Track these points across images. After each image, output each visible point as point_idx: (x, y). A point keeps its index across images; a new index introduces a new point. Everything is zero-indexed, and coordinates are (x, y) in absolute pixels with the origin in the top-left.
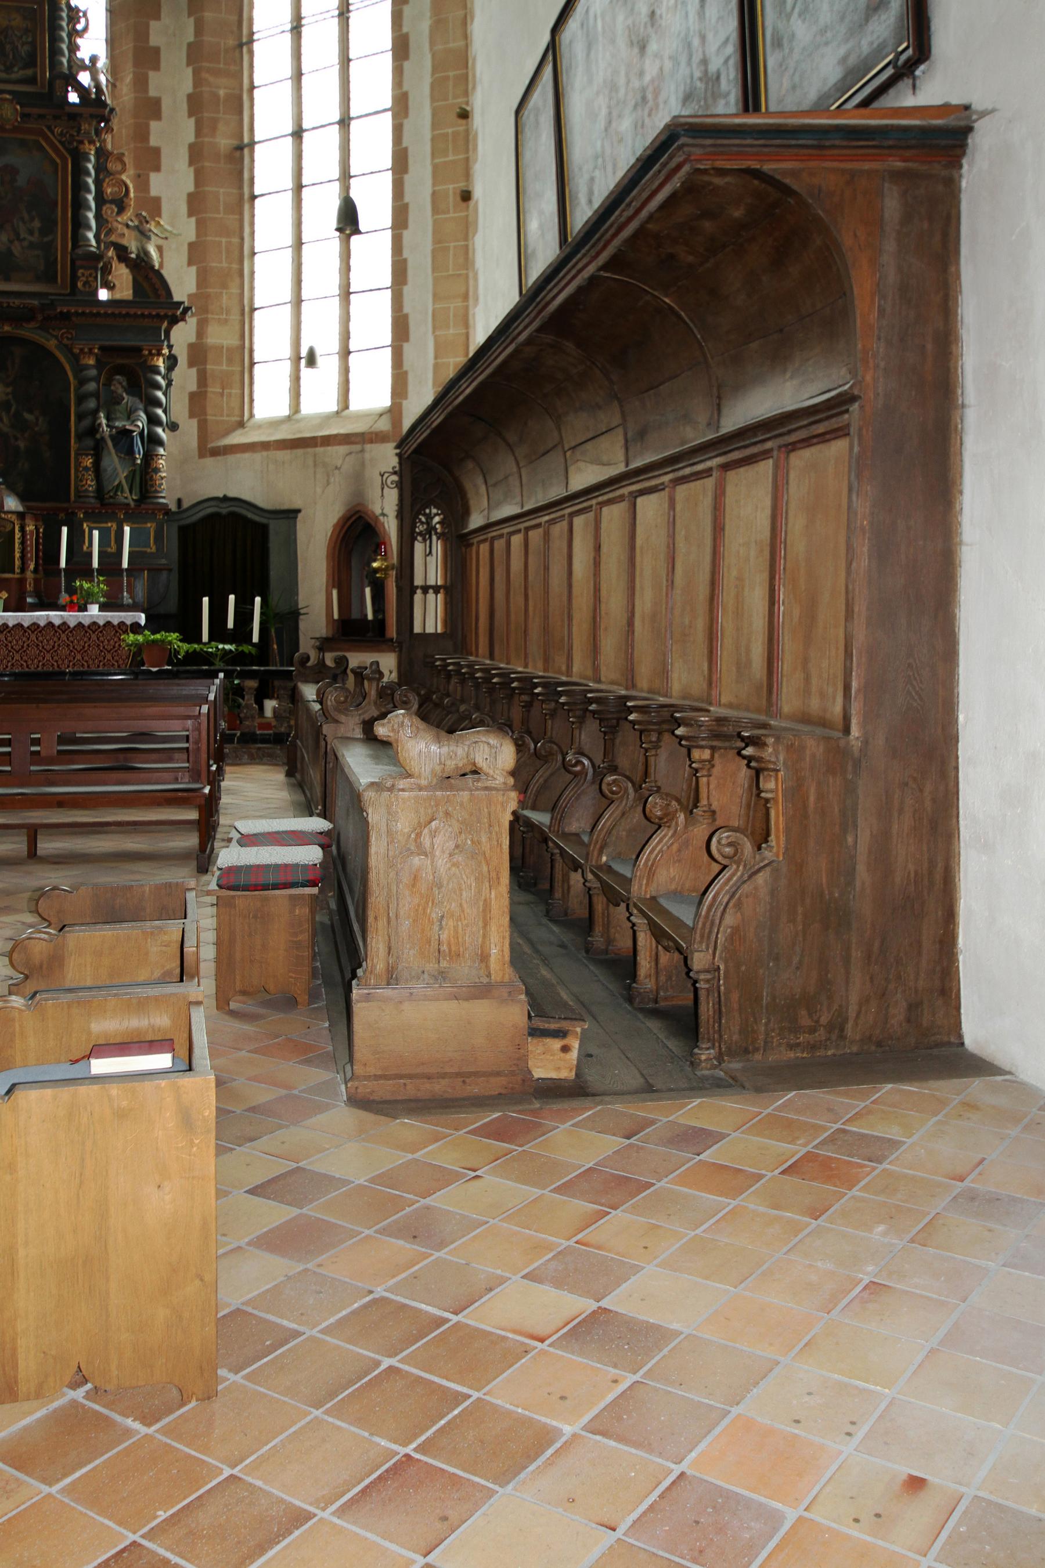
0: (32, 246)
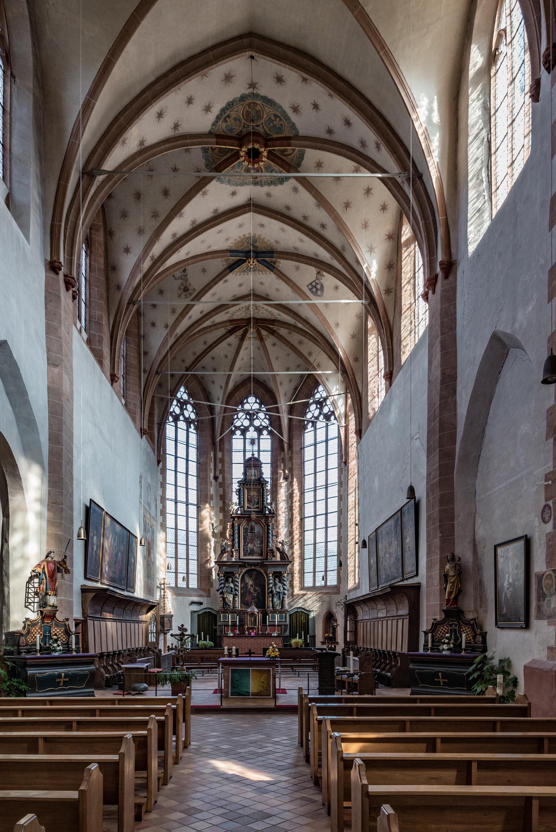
0: (258, 547)
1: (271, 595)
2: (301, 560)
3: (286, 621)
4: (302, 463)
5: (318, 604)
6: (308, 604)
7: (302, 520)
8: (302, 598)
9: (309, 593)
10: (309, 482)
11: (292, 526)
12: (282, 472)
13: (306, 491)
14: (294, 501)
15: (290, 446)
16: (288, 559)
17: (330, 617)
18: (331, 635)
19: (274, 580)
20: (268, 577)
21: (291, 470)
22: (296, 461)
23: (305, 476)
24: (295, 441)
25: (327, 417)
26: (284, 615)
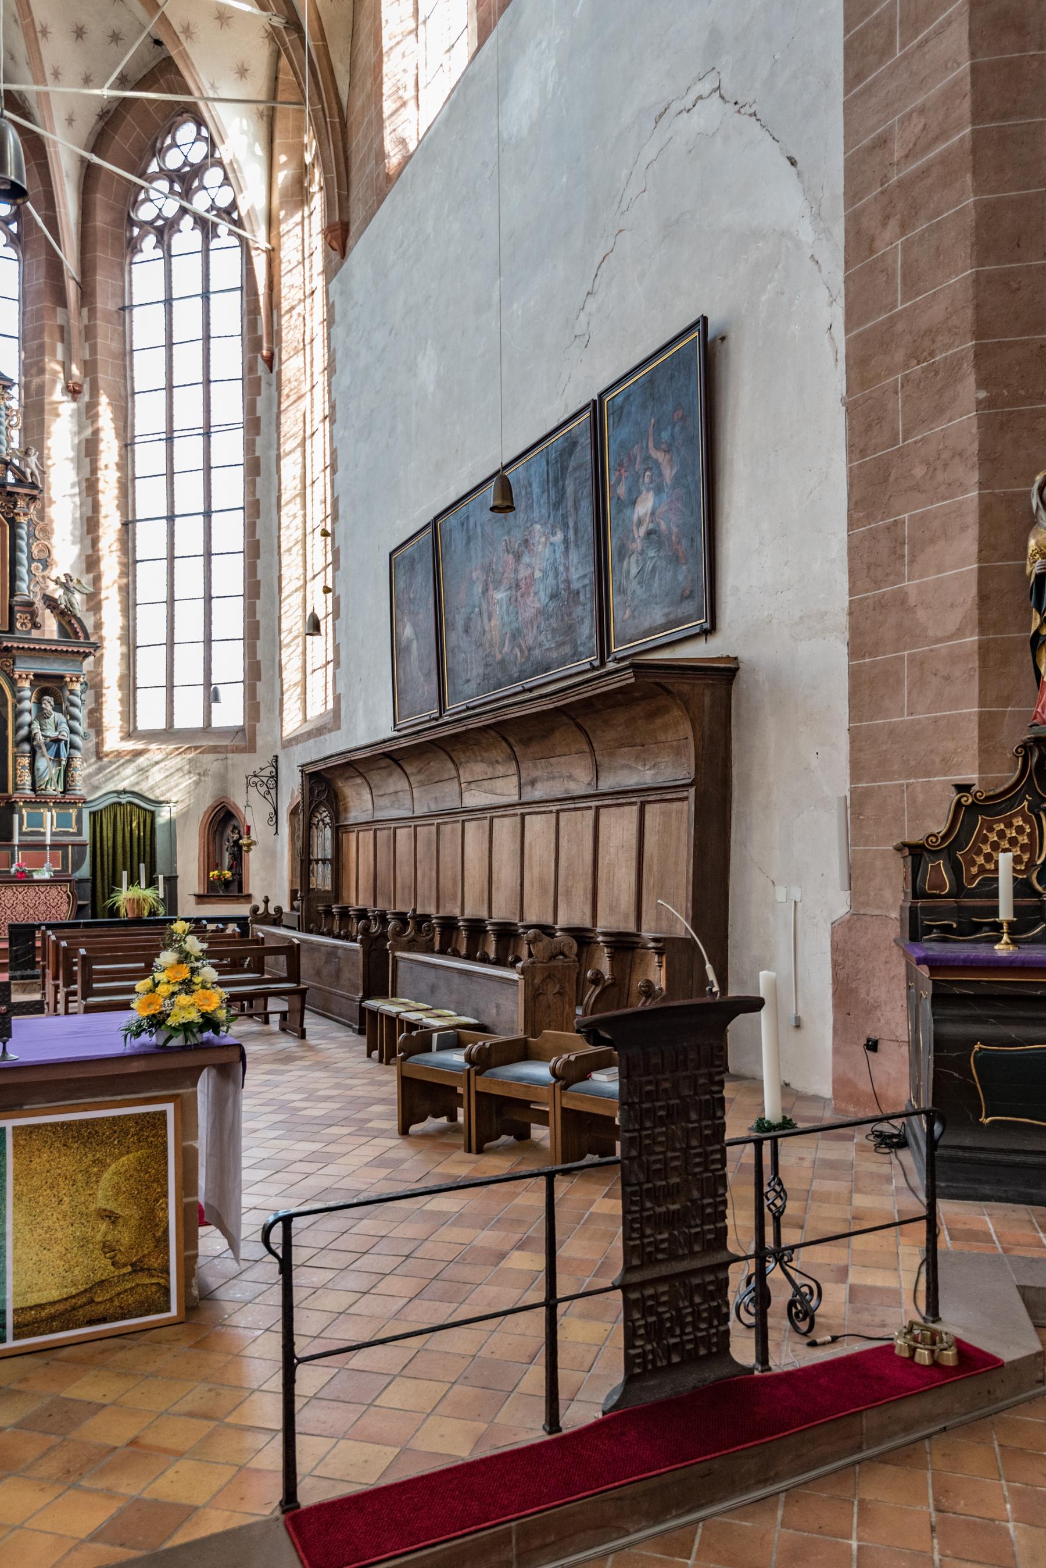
1: (26, 747)
2: (124, 649)
3: (79, 833)
4: (125, 355)
5: (187, 782)
6: (151, 782)
7: (128, 526)
8: (129, 761)
9: (153, 746)
10: (148, 415)
11: (95, 542)
12: (58, 368)
13: (137, 440)
14: (101, 464)
15: (86, 294)
16: (87, 636)
17: (222, 821)
18: (228, 874)
19: (39, 702)
20: (15, 690)
21: (90, 368)
22: (107, 340)
23: (133, 393)
24: (102, 280)
25: (206, 228)
26: (73, 812)
